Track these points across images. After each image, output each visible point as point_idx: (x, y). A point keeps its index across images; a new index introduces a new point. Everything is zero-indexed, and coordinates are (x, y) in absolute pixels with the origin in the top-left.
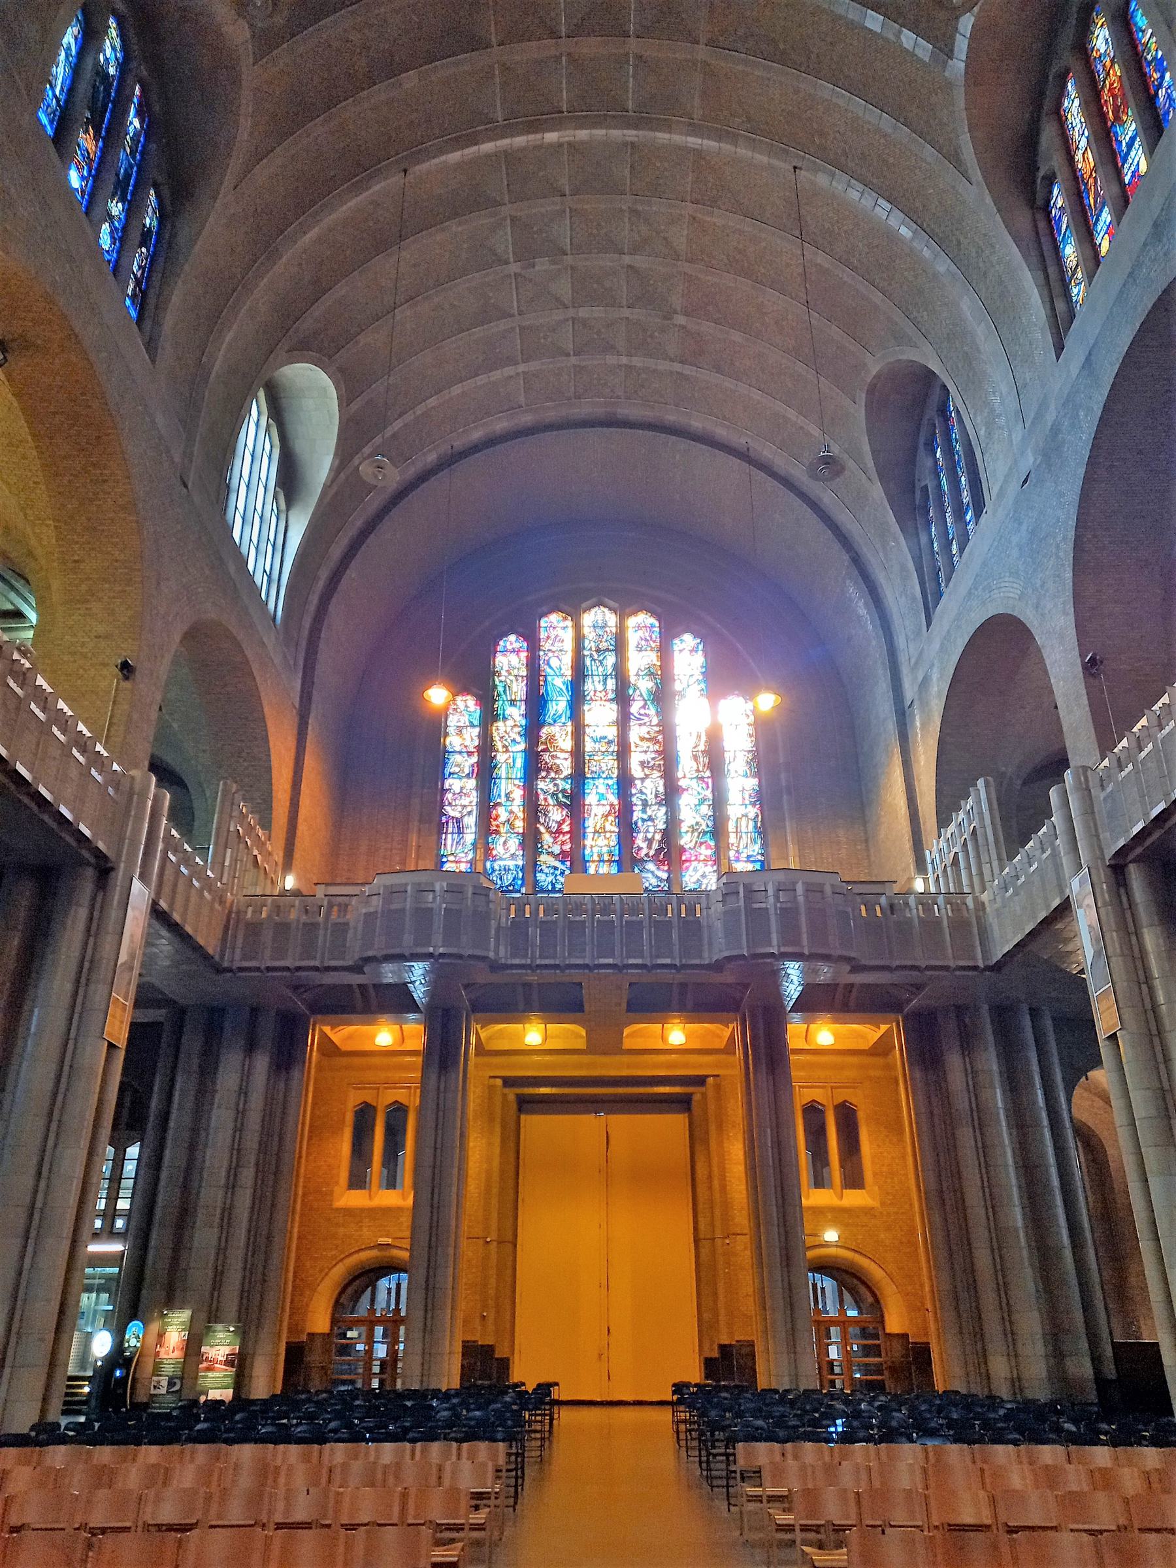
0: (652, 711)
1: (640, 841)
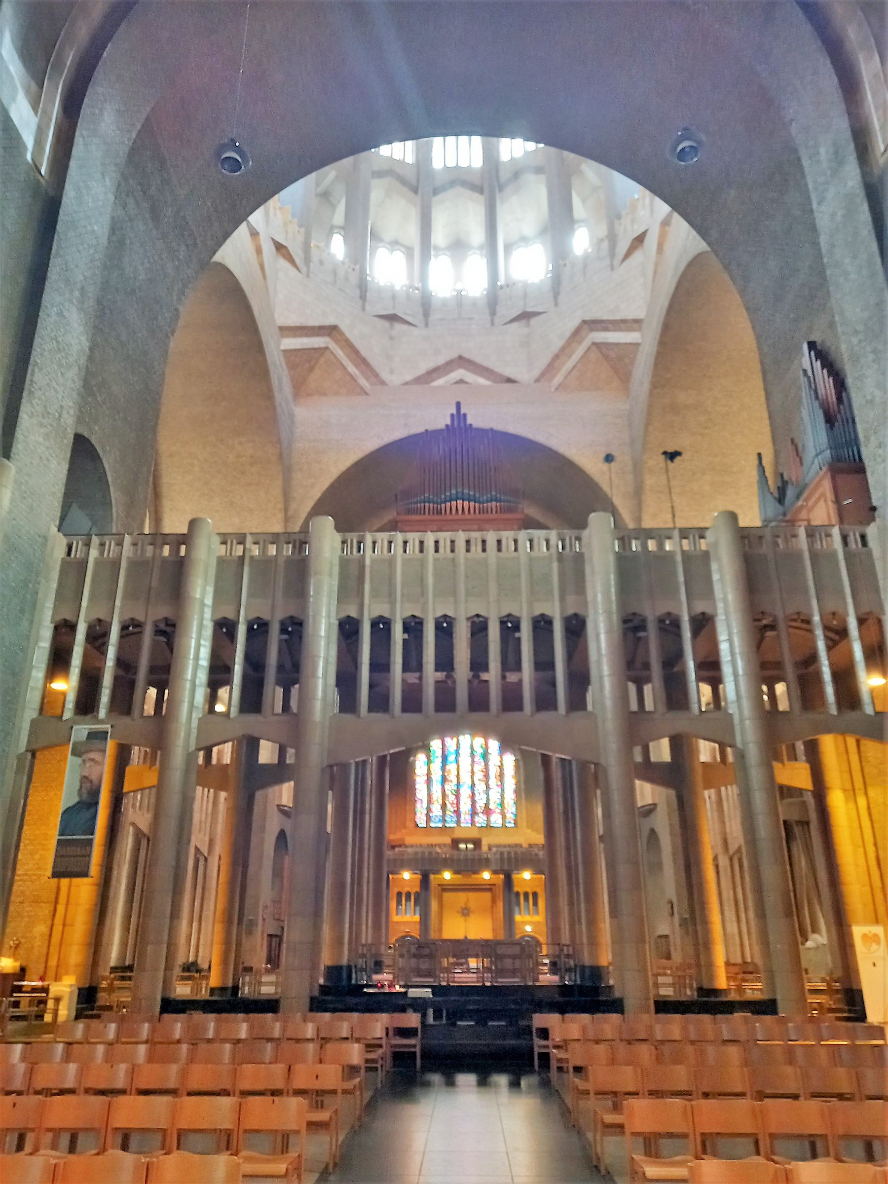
0: (482, 761)
1: (478, 807)
